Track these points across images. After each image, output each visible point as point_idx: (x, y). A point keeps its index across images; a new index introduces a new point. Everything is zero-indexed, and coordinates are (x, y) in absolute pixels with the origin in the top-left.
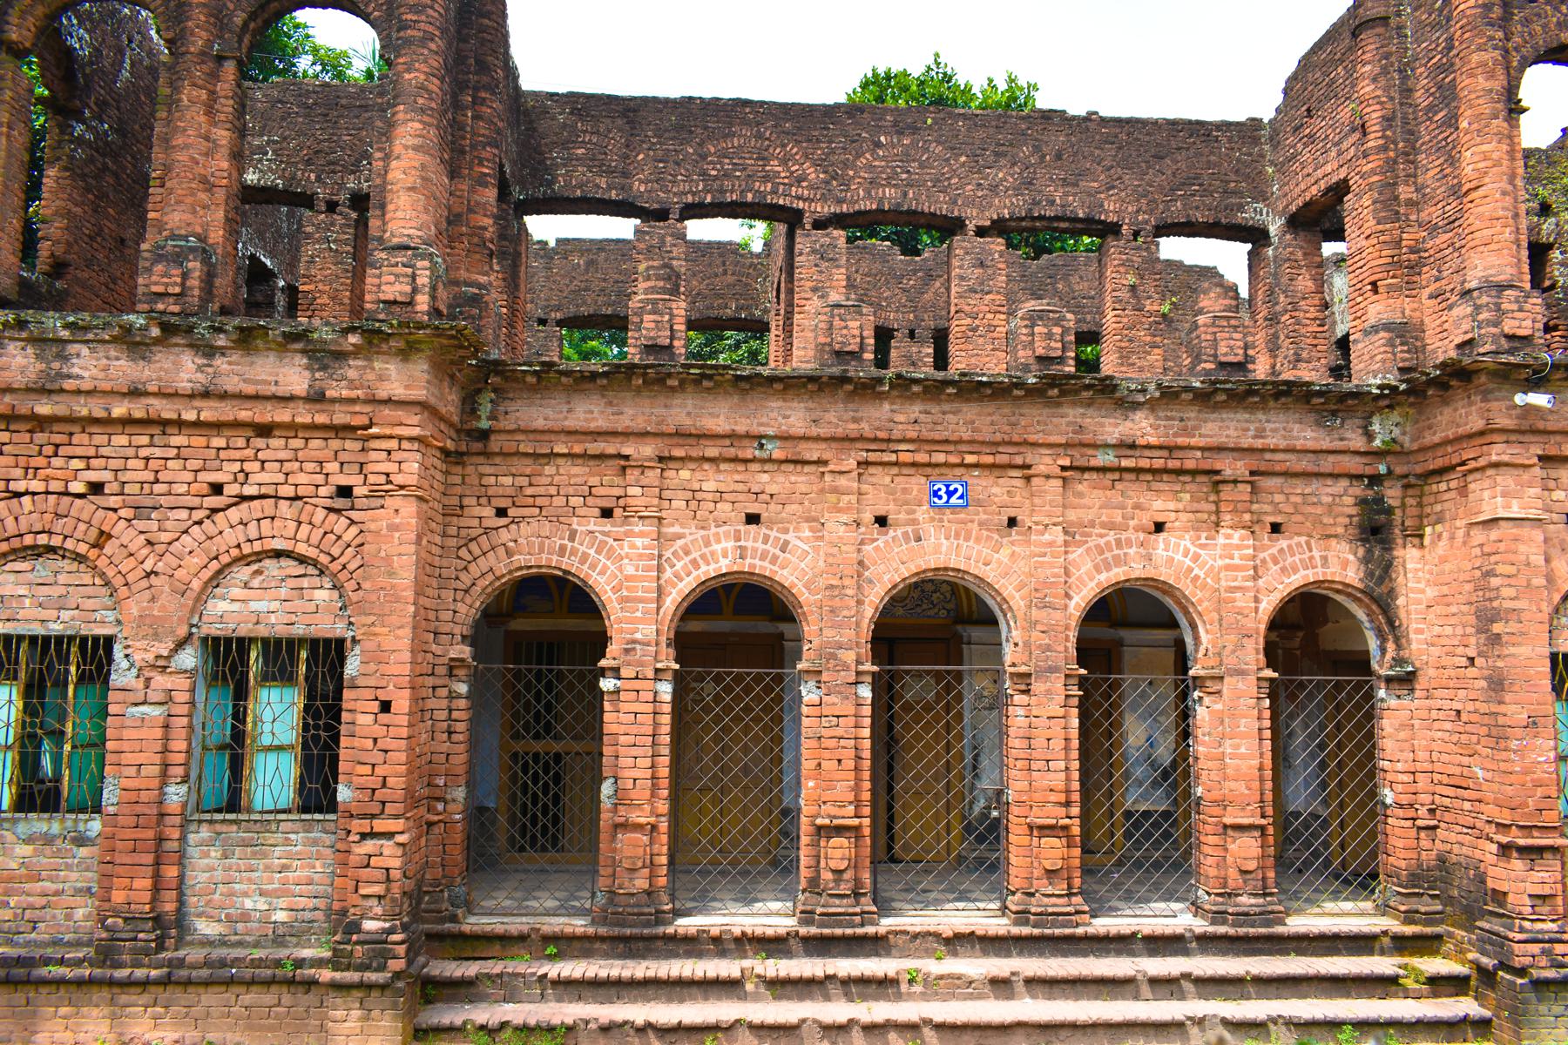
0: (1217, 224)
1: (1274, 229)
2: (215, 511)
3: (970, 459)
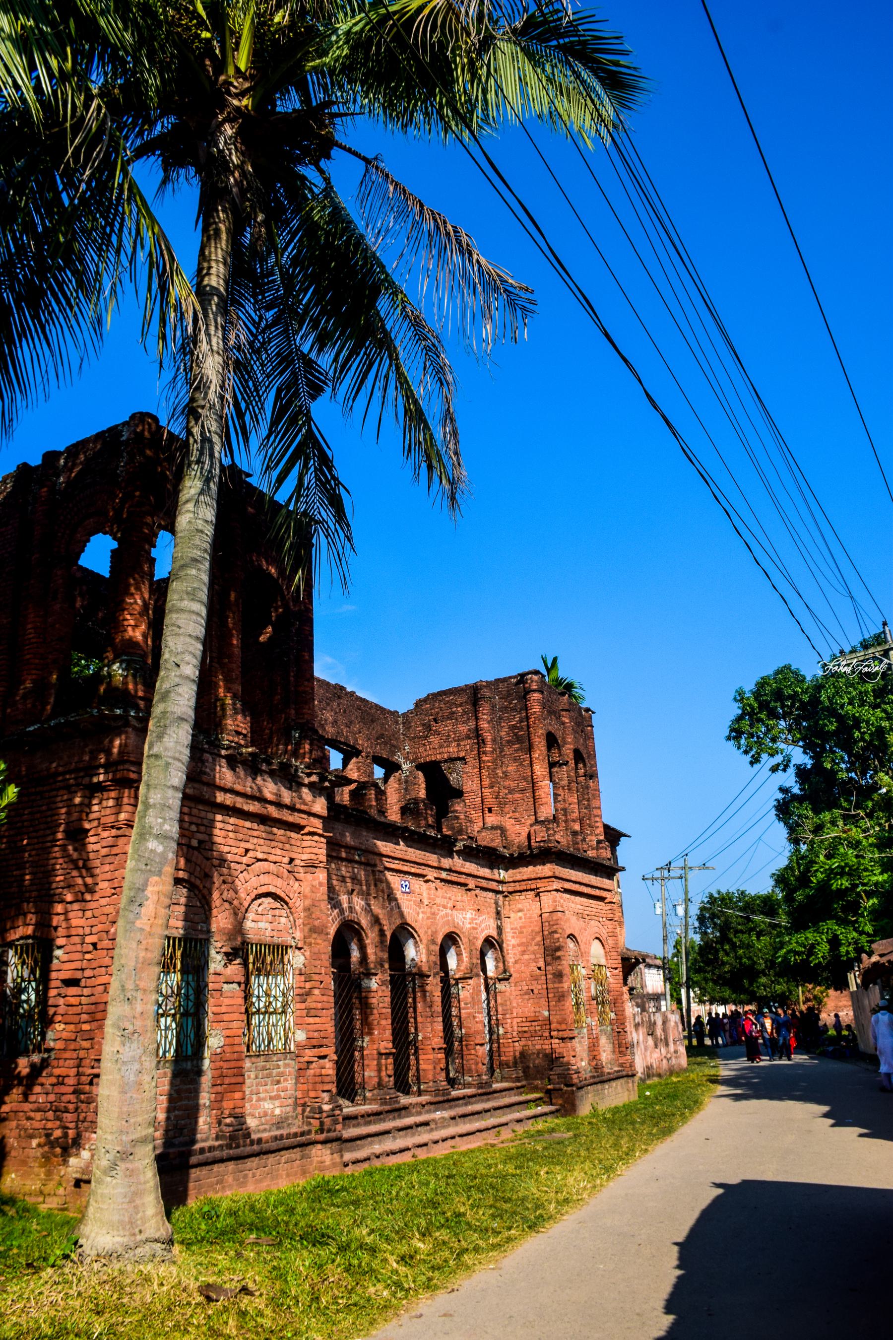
0: (387, 760)
1: (405, 767)
2: (248, 866)
3: (413, 870)
